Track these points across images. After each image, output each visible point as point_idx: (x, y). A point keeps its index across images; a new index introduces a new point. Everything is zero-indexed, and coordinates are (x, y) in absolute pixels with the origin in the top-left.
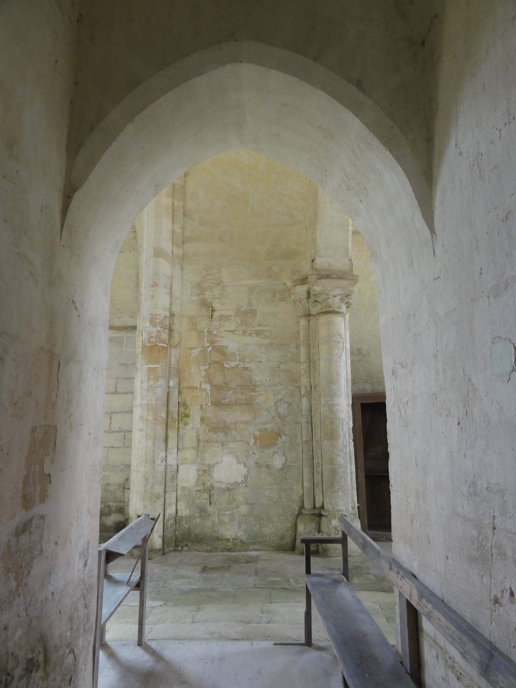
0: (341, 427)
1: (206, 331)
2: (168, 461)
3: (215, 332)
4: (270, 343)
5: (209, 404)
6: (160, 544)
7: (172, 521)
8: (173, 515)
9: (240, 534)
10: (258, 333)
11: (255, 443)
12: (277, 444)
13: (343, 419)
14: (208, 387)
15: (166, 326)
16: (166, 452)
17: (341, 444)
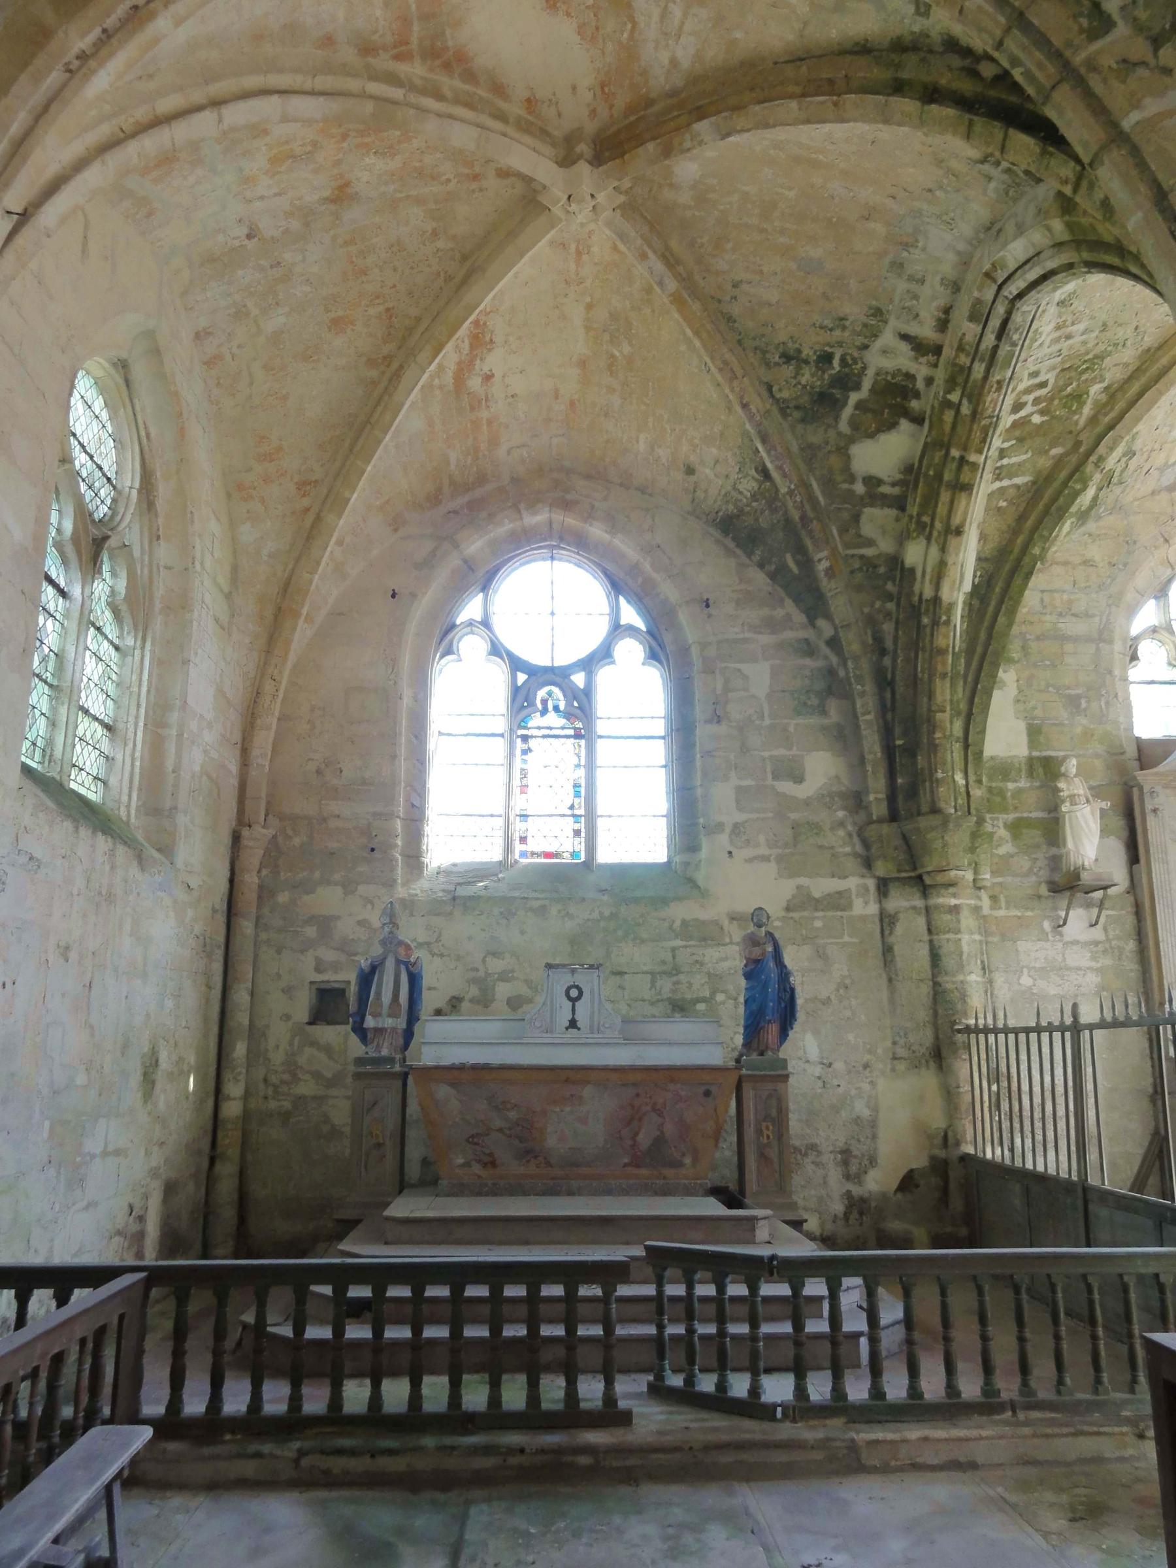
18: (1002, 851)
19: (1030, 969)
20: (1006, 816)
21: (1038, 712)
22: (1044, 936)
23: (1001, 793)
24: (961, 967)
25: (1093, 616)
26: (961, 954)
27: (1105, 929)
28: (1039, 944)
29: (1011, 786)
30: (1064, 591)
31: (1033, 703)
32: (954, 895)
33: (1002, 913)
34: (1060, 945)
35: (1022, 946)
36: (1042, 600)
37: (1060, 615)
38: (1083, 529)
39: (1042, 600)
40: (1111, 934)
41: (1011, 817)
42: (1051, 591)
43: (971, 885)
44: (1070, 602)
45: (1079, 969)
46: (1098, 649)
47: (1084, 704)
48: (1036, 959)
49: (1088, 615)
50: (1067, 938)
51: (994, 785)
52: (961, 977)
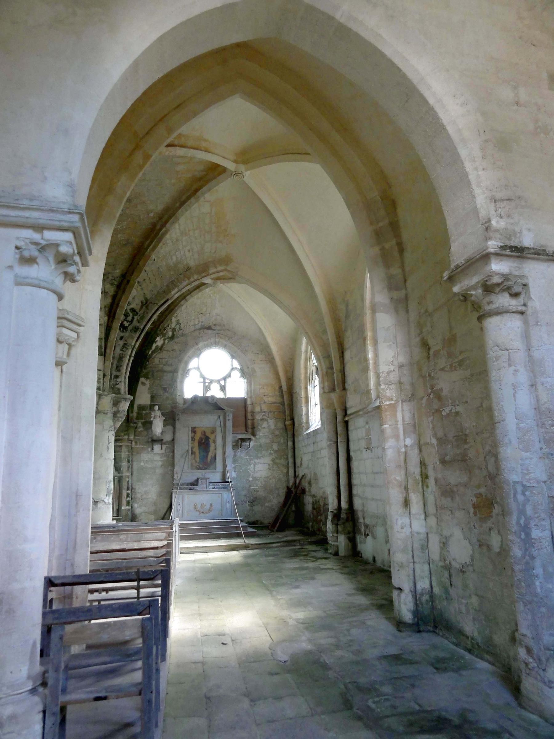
0: (512, 496)
1: (427, 375)
2: (413, 526)
3: (433, 375)
4: (470, 375)
5: (438, 463)
6: (410, 618)
7: (427, 597)
8: (428, 590)
9: (476, 634)
10: (461, 363)
11: (475, 514)
12: (492, 517)
13: (515, 482)
14: (434, 441)
15: (390, 382)
16: (410, 519)
17: (514, 523)
18: (139, 430)
19: (143, 461)
20: (142, 420)
21: (155, 392)
22: (148, 452)
23: (141, 414)
24: (121, 461)
25: (173, 365)
26: (121, 458)
27: (165, 450)
28: (147, 454)
29: (144, 412)
30: (166, 358)
31: (153, 389)
32: (121, 443)
33: (138, 446)
34: (152, 454)
35: (142, 455)
36: (159, 361)
37: (164, 365)
38: (173, 341)
39: (159, 361)
40: (167, 451)
41: (143, 420)
42: (162, 358)
43: (127, 439)
44: (167, 361)
45: (157, 460)
46: (173, 375)
47: (167, 389)
48: (145, 459)
49: (171, 365)
50: (154, 452)
51: (140, 412)
52: (121, 464)
